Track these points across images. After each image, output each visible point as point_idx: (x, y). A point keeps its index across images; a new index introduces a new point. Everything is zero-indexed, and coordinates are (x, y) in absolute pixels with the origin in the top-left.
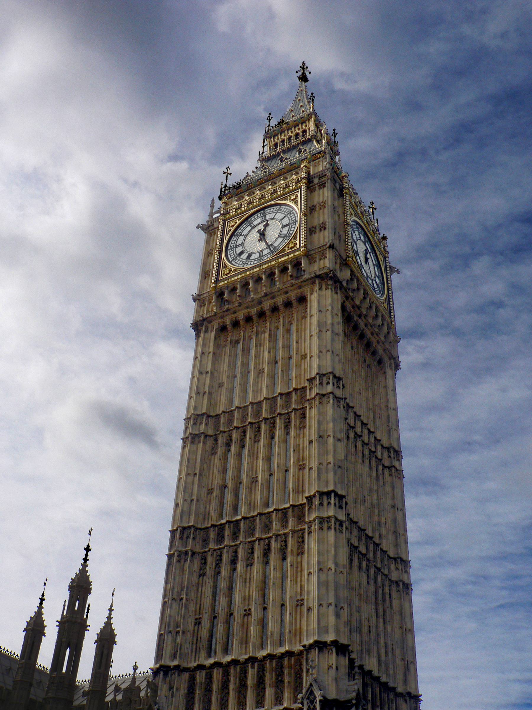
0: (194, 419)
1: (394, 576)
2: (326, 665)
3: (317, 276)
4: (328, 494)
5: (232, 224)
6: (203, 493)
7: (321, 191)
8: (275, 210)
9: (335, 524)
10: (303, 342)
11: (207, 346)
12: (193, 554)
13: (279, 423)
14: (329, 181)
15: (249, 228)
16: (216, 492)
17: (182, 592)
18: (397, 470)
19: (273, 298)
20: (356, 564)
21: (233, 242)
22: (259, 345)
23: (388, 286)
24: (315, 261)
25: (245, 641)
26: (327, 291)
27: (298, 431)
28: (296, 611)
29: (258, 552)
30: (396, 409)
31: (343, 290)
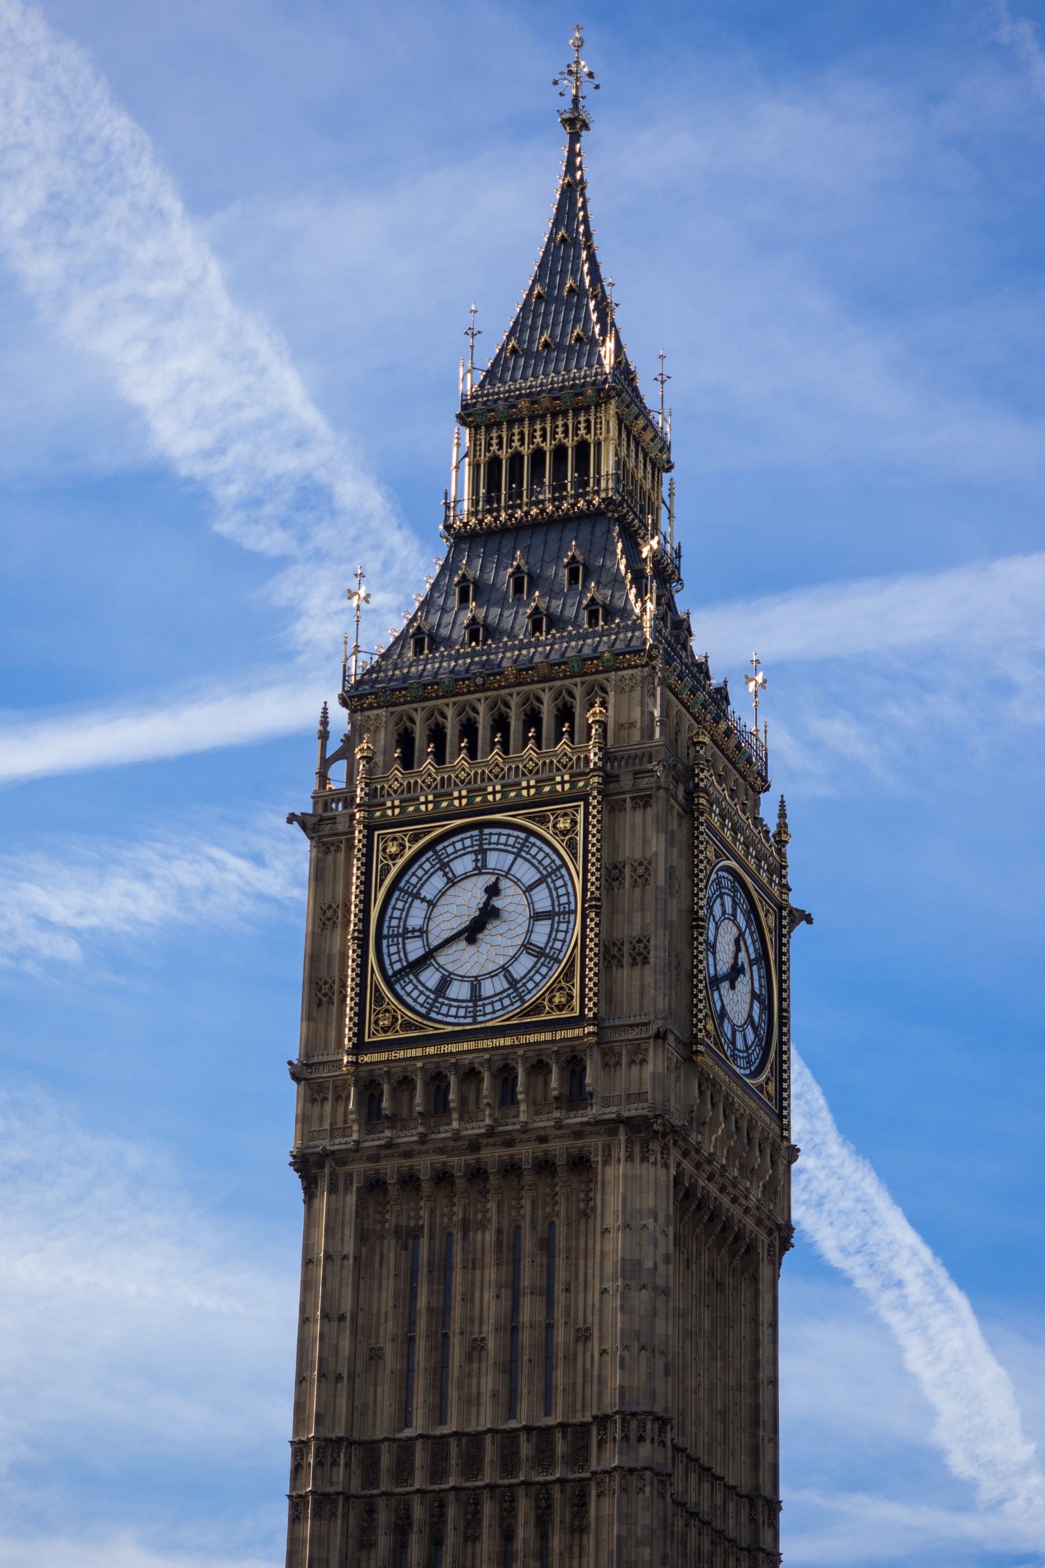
3: (621, 1121)
5: (393, 849)
7: (639, 813)
8: (511, 841)
10: (581, 1288)
11: (338, 1236)
13: (524, 1508)
14: (662, 792)
15: (438, 881)
19: (510, 1143)
21: (397, 914)
22: (473, 1264)
23: (781, 1010)
24: (618, 1064)
26: (645, 1164)
30: (774, 1382)
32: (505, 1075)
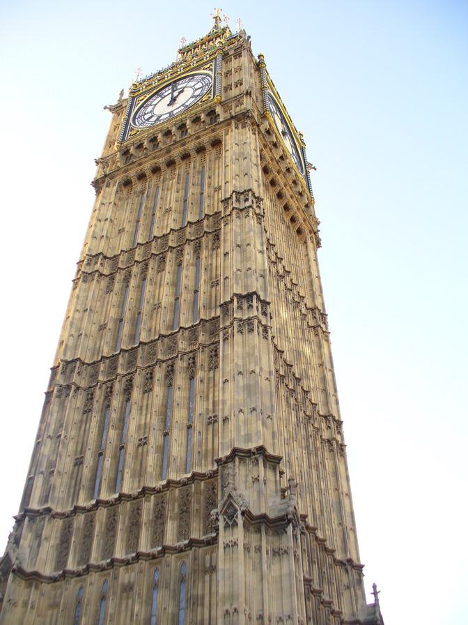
0: (88, 260)
1: (326, 435)
2: (250, 477)
4: (249, 297)
6: (93, 329)
7: (237, 60)
9: (258, 328)
12: (78, 388)
13: (188, 249)
16: (110, 325)
17: (61, 429)
18: (324, 332)
20: (283, 394)
25: (140, 473)
27: (210, 252)
28: (207, 430)
29: (159, 373)
30: (318, 277)
31: (261, 136)
32: (182, 127)
